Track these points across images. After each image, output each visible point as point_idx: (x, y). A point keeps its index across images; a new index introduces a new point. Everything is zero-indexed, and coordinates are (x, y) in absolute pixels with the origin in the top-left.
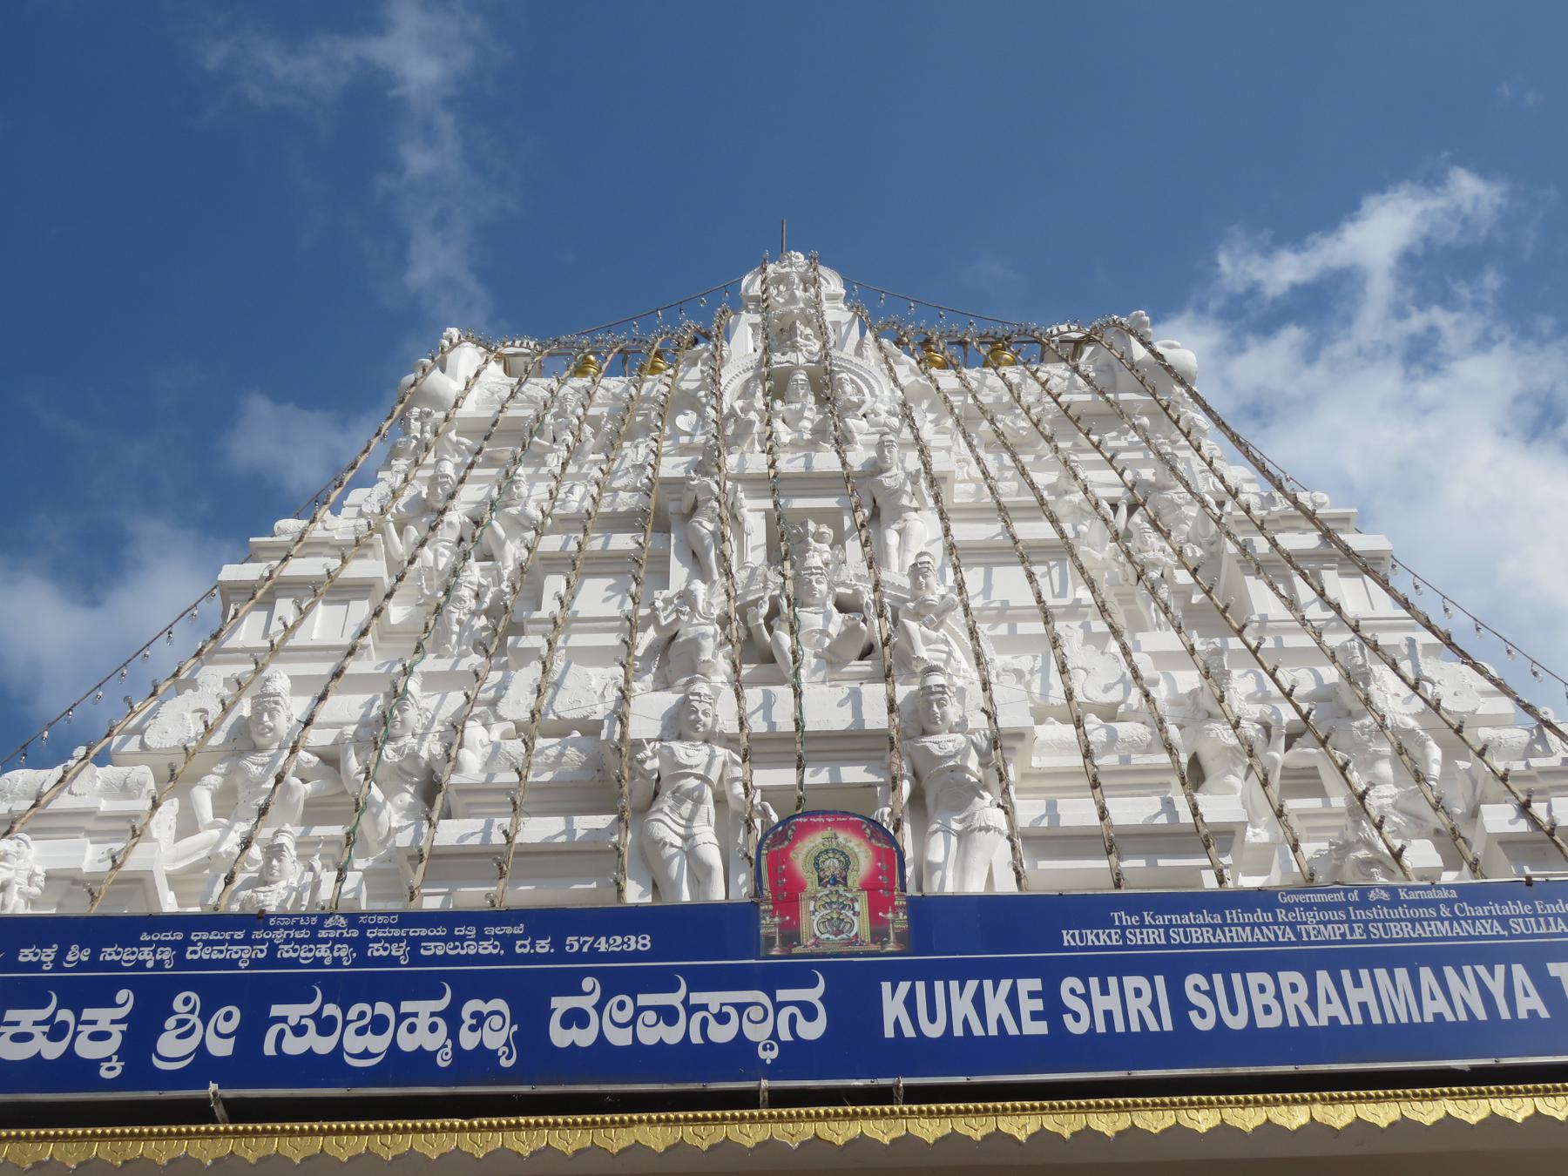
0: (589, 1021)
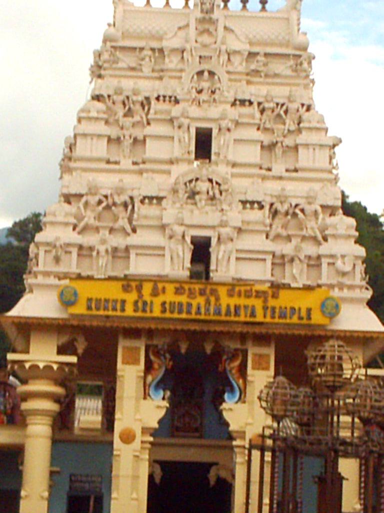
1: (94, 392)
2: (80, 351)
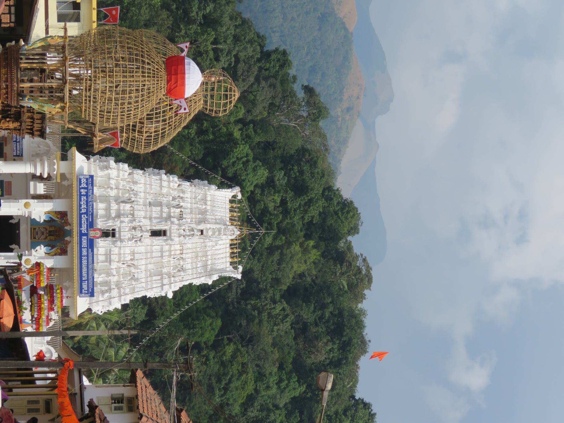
0: (84, 218)
1: (47, 189)
2: (64, 183)
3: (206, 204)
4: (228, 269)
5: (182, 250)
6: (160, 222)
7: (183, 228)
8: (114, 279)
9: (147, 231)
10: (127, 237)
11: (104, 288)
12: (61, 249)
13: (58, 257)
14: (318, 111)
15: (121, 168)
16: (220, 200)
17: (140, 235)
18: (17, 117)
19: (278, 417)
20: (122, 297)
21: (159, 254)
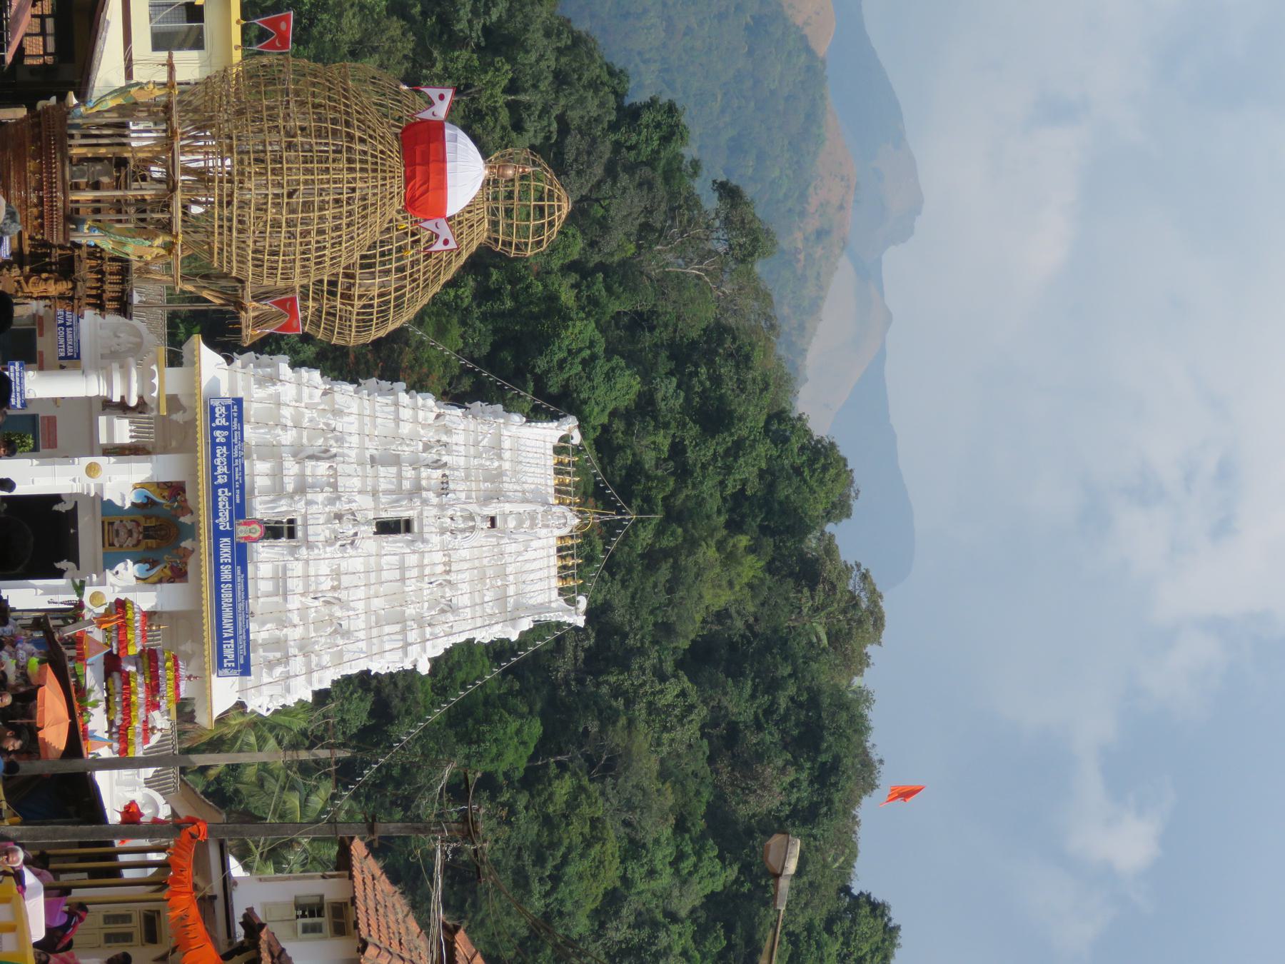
0: (223, 495)
1: (137, 433)
2: (175, 417)
3: (500, 458)
4: (554, 605)
5: (448, 564)
6: (397, 501)
7: (450, 512)
8: (295, 634)
9: (368, 523)
10: (322, 538)
11: (272, 656)
12: (172, 568)
13: (166, 586)
14: (750, 240)
15: (305, 380)
16: (532, 447)
17: (352, 532)
18: (66, 269)
19: (676, 938)
20: (315, 675)
21: (397, 574)
